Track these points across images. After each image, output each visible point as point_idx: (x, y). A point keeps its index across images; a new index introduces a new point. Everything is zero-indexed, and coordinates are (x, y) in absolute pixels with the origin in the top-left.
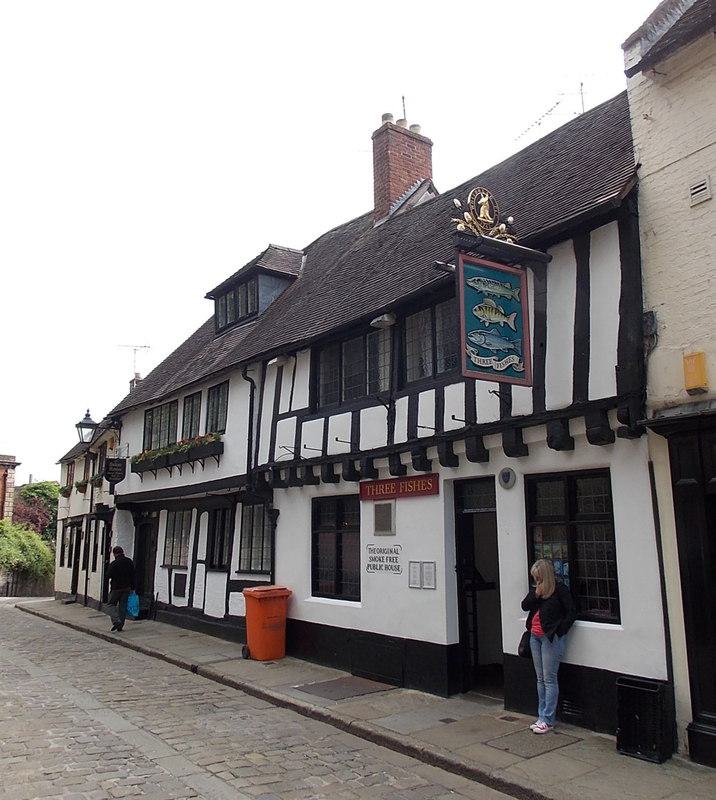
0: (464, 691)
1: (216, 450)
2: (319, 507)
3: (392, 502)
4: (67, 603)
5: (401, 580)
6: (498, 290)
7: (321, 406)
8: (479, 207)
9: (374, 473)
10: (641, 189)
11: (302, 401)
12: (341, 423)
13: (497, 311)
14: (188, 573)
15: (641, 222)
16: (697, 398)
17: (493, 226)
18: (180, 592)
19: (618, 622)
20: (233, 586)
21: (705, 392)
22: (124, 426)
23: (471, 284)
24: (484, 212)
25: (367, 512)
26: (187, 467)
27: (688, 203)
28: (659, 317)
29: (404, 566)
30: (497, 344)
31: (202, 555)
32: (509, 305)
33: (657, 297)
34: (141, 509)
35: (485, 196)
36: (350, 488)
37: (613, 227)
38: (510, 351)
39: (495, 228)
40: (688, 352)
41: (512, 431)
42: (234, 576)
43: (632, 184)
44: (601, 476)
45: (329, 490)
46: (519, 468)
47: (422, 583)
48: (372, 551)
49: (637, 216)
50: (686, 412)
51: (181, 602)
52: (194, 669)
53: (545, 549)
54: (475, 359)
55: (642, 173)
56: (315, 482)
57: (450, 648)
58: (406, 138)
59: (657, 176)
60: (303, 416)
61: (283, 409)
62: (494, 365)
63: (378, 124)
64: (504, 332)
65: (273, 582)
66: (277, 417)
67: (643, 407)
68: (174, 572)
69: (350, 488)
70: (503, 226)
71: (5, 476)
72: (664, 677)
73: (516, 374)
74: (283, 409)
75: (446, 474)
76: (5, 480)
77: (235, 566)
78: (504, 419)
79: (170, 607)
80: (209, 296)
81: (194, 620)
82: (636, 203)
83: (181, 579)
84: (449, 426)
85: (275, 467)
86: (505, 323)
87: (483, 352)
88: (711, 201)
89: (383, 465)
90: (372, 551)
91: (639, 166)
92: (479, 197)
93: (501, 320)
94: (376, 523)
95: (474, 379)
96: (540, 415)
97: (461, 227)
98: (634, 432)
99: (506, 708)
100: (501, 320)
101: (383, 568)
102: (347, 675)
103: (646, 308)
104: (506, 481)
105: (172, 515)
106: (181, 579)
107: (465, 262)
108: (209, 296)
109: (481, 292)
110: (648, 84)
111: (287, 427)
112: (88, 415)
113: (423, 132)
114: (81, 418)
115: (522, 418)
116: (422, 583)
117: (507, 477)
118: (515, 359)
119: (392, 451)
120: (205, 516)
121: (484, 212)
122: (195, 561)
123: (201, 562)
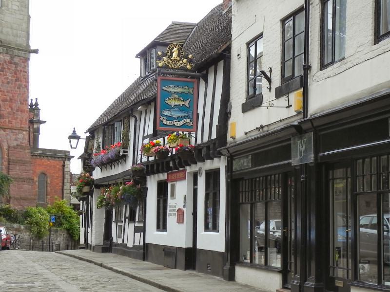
3: (175, 183)
6: (180, 90)
8: (172, 54)
13: (179, 100)
14: (123, 224)
17: (179, 61)
18: (118, 236)
24: (175, 55)
31: (128, 215)
32: (183, 96)
35: (176, 47)
37: (213, 67)
38: (185, 117)
39: (180, 62)
42: (137, 225)
43: (228, 44)
48: (170, 207)
51: (120, 241)
54: (164, 122)
55: (233, 38)
61: (146, 135)
62: (176, 124)
64: (181, 108)
66: (144, 138)
67: (227, 143)
71: (64, 166)
74: (146, 135)
75: (188, 169)
76: (63, 169)
77: (137, 220)
79: (117, 245)
80: (137, 56)
81: (124, 251)
82: (230, 52)
86: (183, 104)
87: (168, 118)
90: (170, 207)
92: (173, 48)
93: (181, 103)
97: (160, 65)
100: (181, 103)
107: (161, 79)
108: (137, 56)
112: (74, 131)
114: (70, 133)
118: (188, 120)
121: (175, 55)
122: (126, 218)
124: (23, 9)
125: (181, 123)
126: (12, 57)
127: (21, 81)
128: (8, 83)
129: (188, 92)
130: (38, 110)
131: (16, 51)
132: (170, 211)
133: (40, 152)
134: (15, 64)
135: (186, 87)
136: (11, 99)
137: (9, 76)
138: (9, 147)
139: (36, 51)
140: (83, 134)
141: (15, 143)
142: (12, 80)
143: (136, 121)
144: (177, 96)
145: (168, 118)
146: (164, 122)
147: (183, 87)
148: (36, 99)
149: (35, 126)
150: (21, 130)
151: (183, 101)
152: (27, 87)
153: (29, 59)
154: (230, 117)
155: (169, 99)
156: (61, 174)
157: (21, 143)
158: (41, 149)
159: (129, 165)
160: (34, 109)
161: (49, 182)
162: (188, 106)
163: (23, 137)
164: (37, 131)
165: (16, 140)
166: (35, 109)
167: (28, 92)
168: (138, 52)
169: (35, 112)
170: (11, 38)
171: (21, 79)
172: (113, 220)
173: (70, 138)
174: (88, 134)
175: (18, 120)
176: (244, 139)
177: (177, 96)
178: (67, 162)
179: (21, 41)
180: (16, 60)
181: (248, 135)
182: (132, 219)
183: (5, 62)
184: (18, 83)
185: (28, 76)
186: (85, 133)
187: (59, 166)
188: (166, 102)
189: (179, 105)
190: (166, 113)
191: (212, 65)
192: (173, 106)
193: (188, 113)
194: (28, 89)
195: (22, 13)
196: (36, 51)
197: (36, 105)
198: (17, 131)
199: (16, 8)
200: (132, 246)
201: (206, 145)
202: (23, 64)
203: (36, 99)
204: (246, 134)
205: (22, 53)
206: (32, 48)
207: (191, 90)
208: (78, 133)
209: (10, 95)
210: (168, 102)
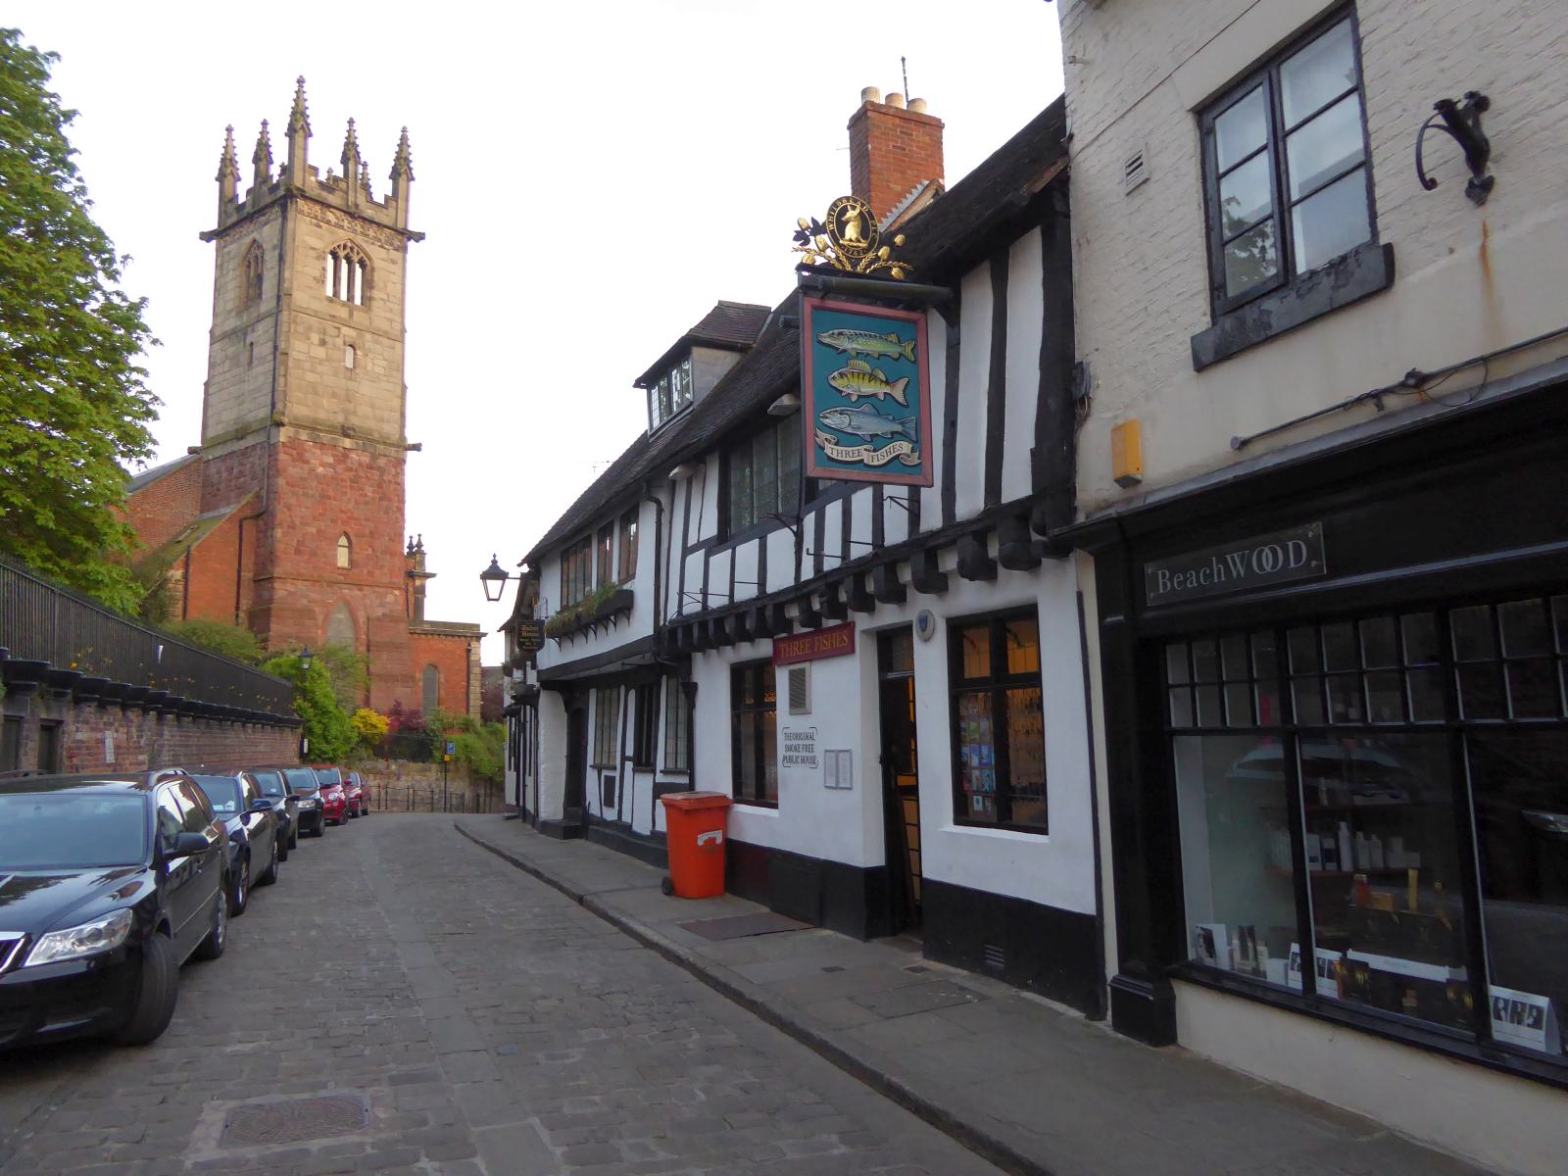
0: (894, 933)
1: (620, 606)
2: (738, 672)
4: (508, 818)
5: (817, 775)
6: (875, 346)
7: (733, 532)
8: (842, 226)
9: (787, 625)
10: (1073, 173)
11: (710, 529)
12: (748, 551)
13: (872, 377)
14: (617, 774)
15: (1074, 224)
16: (1130, 492)
17: (866, 251)
18: (608, 801)
19: (1044, 831)
20: (658, 790)
21: (1138, 482)
22: (543, 574)
23: (827, 340)
24: (851, 232)
25: (782, 678)
26: (601, 631)
27: (1123, 189)
28: (1093, 370)
29: (820, 759)
30: (871, 425)
31: (630, 752)
32: (886, 367)
33: (1096, 341)
34: (569, 686)
35: (854, 208)
36: (764, 648)
38: (894, 436)
39: (871, 255)
40: (1120, 422)
41: (924, 548)
42: (660, 778)
43: (1059, 166)
44: (1028, 613)
45: (747, 652)
46: (937, 609)
47: (837, 782)
48: (788, 736)
49: (1068, 216)
50: (1121, 509)
51: (610, 815)
52: (581, 900)
53: (972, 728)
54: (831, 450)
55: (1076, 146)
56: (730, 641)
57: (870, 873)
58: (897, 121)
59: (1091, 150)
60: (712, 547)
61: (692, 541)
62: (867, 457)
63: (855, 105)
65: (691, 787)
66: (687, 551)
67: (1073, 510)
68: (605, 773)
69: (764, 648)
70: (884, 251)
71: (469, 651)
72: (1090, 909)
73: (909, 470)
74: (692, 541)
75: (862, 622)
76: (468, 657)
77: (660, 765)
78: (914, 537)
79: (602, 822)
80: (638, 384)
82: (1066, 196)
83: (610, 781)
84: (857, 552)
85: (684, 623)
87: (843, 437)
88: (1148, 183)
89: (793, 612)
90: (788, 736)
91: (1071, 137)
93: (881, 390)
94: (791, 700)
95: (881, 484)
96: (953, 531)
98: (1060, 549)
99: (925, 957)
100: (881, 390)
101: (799, 760)
102: (765, 909)
103: (1078, 358)
104: (924, 629)
105: (600, 695)
106: (610, 781)
107: (815, 308)
108: (638, 384)
109: (844, 351)
110: (1080, 9)
111: (696, 559)
112: (494, 562)
113: (929, 110)
114: (486, 566)
115: (933, 534)
116: (837, 782)
117: (924, 621)
118: (905, 447)
119: (800, 592)
120: (632, 694)
121: (851, 232)
122: (624, 758)
123: (629, 759)
124: (394, 373)
125: (881, 458)
126: (374, 457)
127: (390, 500)
128: (366, 503)
129: (901, 354)
130: (423, 554)
131: (382, 447)
132: (789, 748)
133: (426, 627)
134: (379, 468)
135: (893, 338)
136: (371, 532)
137: (369, 491)
138: (368, 619)
139: (417, 447)
140: (516, 570)
141: (379, 612)
142: (373, 498)
143: (660, 512)
144: (867, 368)
145: (843, 437)
146: (828, 451)
147: (882, 336)
148: (420, 535)
149: (418, 582)
150: (392, 587)
151: (887, 383)
152: (401, 510)
153: (404, 461)
154: (1088, 415)
155: (842, 375)
156: (464, 665)
157: (391, 611)
158: (427, 622)
159: (641, 626)
160: (414, 554)
161: (442, 680)
162: (901, 399)
163: (394, 598)
164: (421, 591)
165: (382, 605)
166: (417, 552)
167: (403, 520)
168: (640, 374)
169: (418, 558)
170: (371, 424)
171: (391, 498)
172: (590, 761)
173: (485, 576)
174: (525, 569)
175: (386, 570)
176: (1208, 475)
177: (867, 368)
178: (474, 644)
179: (390, 429)
180: (382, 462)
181: (1256, 449)
182: (644, 761)
183: (360, 464)
184: (385, 503)
185: (403, 491)
186: (519, 565)
187: (461, 652)
188: (833, 383)
189: (874, 395)
190: (834, 420)
191: (1026, 229)
192: (854, 399)
193: (902, 424)
194: (403, 515)
195: (392, 380)
196: (417, 447)
197: (419, 545)
198: (381, 590)
199: (382, 371)
200: (647, 832)
201: (974, 528)
202: (393, 470)
203: (420, 535)
204: (1244, 443)
205: (392, 451)
206: (411, 440)
207: (909, 349)
208: (503, 566)
209: (372, 525)
210: (838, 383)
